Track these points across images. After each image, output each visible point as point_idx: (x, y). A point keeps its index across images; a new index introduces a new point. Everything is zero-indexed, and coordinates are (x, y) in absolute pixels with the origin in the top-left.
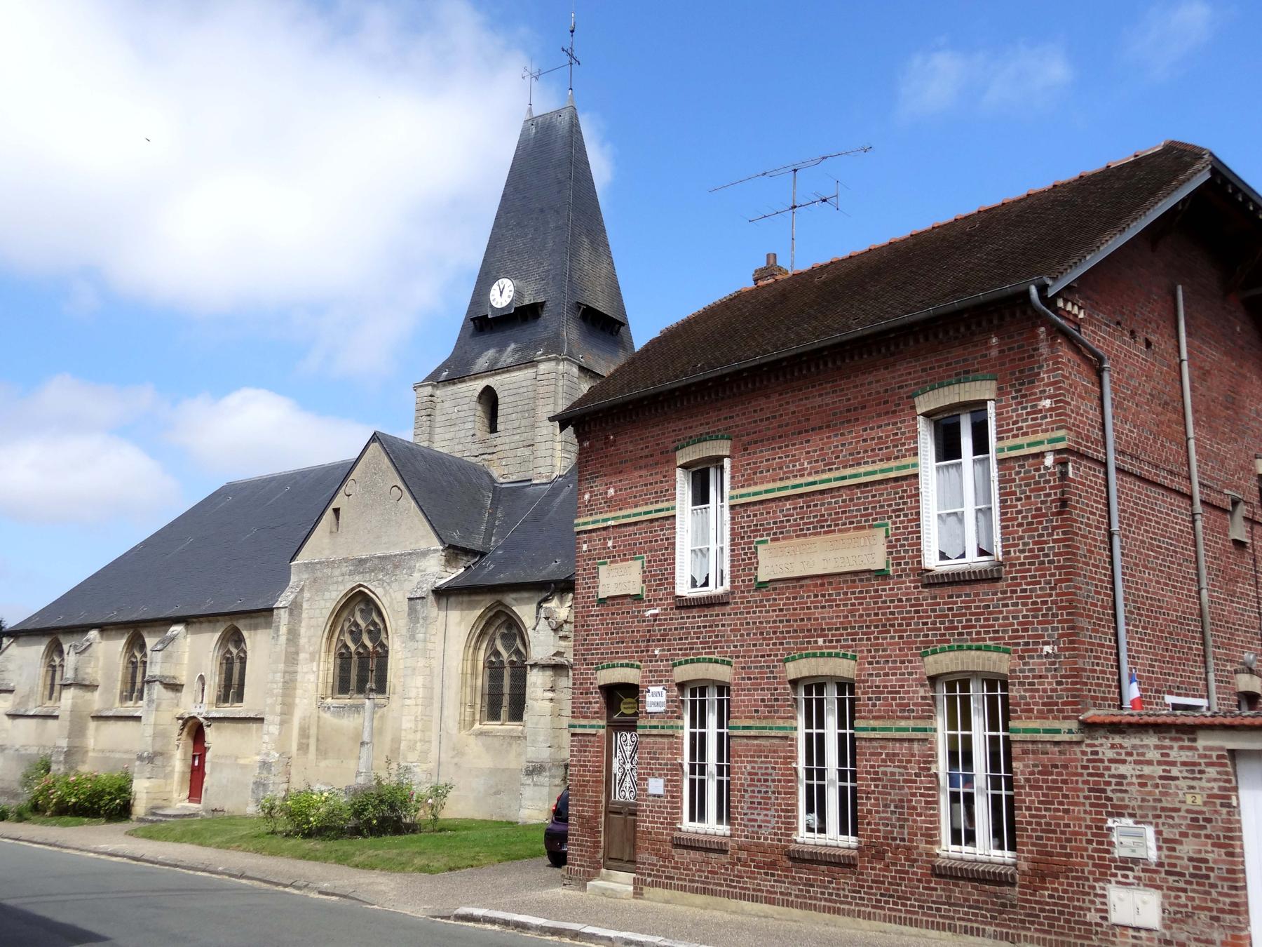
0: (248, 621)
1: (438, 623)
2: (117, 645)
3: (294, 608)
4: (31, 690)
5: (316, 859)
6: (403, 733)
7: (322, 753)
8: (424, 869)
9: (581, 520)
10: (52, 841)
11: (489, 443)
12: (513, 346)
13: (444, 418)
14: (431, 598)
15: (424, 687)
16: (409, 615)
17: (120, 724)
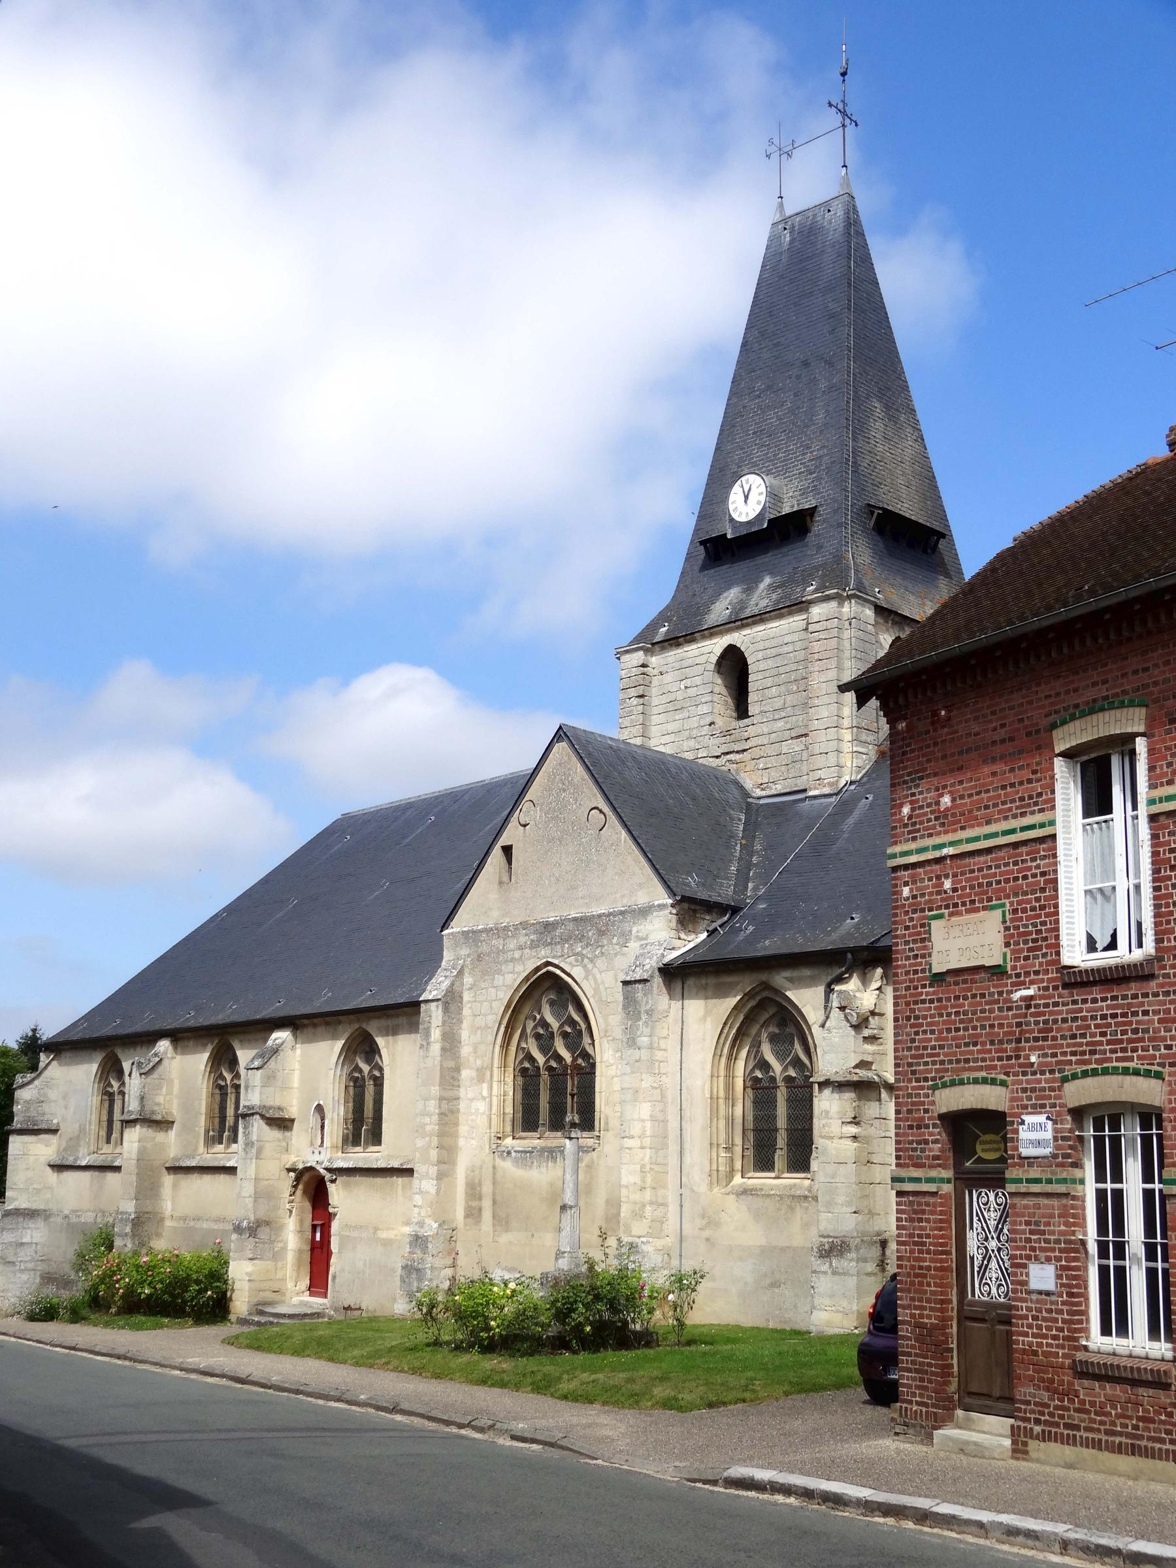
0: (383, 1022)
1: (670, 1020)
2: (199, 1060)
3: (451, 1000)
4: (82, 1129)
5: (503, 1385)
6: (624, 1192)
7: (502, 1222)
8: (668, 1404)
9: (897, 849)
10: (121, 1350)
11: (736, 734)
12: (767, 580)
13: (665, 699)
14: (658, 980)
15: (653, 1119)
16: (625, 1007)
17: (207, 1179)
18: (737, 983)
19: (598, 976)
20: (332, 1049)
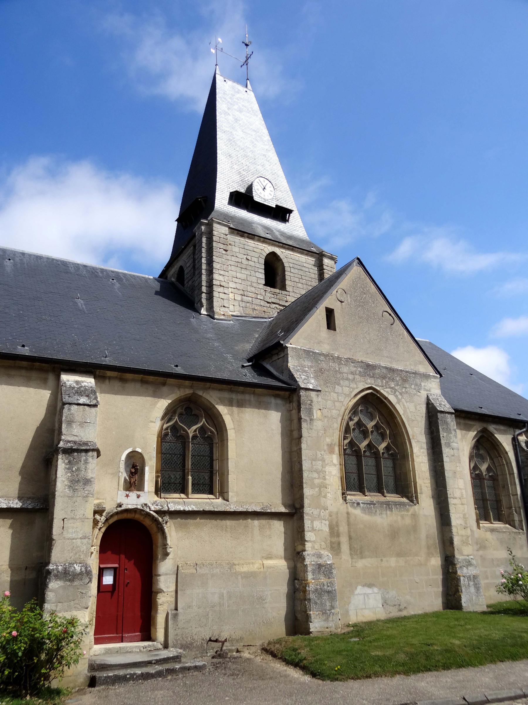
7: (357, 552)
18: (474, 425)
19: (405, 404)
20: (155, 404)
